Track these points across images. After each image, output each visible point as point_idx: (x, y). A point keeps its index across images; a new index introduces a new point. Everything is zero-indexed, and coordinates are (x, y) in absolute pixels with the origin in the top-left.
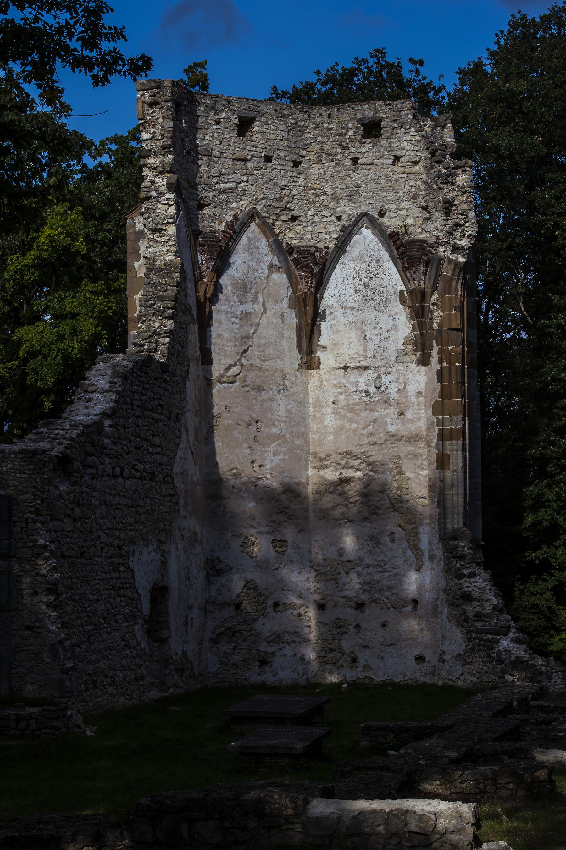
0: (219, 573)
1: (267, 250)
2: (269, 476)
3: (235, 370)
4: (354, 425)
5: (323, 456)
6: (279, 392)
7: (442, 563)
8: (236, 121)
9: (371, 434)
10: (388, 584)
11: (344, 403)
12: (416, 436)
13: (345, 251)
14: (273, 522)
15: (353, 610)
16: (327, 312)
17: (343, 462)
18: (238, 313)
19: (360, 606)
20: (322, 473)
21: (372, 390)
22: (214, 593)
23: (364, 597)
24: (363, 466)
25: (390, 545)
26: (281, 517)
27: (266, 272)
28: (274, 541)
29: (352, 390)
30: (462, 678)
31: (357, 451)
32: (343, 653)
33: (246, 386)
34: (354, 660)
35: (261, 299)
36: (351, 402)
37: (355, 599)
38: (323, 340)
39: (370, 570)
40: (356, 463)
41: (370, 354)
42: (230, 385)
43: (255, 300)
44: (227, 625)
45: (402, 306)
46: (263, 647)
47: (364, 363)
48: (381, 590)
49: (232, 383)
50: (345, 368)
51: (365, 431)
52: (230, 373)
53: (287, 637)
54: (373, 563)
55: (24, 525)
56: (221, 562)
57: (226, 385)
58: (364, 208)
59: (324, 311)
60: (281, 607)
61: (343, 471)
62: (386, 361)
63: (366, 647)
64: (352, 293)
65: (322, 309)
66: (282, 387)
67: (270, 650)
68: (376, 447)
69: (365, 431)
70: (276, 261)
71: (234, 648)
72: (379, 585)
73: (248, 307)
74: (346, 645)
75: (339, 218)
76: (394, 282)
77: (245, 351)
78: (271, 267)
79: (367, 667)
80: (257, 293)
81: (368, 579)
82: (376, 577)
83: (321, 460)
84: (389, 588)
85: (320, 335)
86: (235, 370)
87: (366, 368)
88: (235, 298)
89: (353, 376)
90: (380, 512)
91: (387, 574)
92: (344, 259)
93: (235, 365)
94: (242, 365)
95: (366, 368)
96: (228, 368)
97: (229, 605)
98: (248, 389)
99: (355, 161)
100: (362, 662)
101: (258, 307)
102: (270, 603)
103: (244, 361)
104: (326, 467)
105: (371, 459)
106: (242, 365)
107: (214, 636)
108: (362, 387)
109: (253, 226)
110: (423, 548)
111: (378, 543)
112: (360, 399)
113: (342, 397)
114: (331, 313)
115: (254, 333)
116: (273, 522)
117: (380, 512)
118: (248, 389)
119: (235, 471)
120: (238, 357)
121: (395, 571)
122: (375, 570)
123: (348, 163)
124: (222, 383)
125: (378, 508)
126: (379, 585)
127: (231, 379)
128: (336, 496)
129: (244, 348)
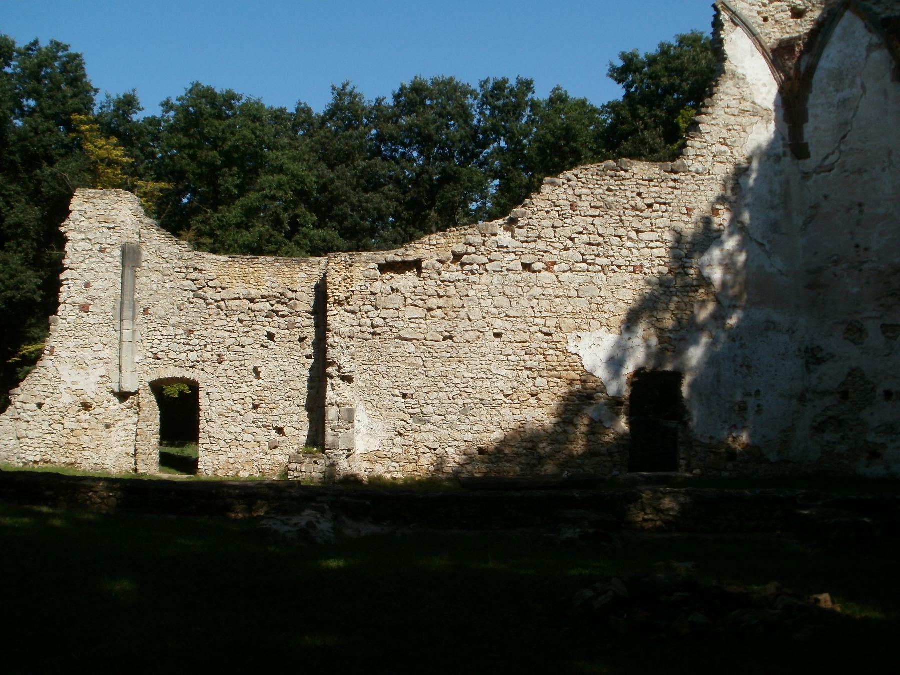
0: (820, 361)
1: (864, 32)
2: (874, 259)
3: (832, 159)
6: (884, 170)
14: (882, 306)
27: (864, 53)
28: (883, 326)
33: (846, 171)
35: (858, 81)
42: (828, 174)
43: (852, 84)
44: (830, 413)
46: (871, 437)
49: (830, 171)
52: (827, 163)
56: (822, 350)
57: (823, 175)
67: (880, 441)
71: (843, 438)
73: (846, 93)
77: (844, 137)
78: (870, 49)
80: (854, 77)
86: (832, 159)
88: (832, 89)
93: (833, 153)
94: (841, 152)
96: (827, 158)
97: (831, 393)
98: (847, 174)
101: (857, 91)
102: (880, 391)
103: (843, 148)
106: (841, 152)
109: (848, 14)
115: (853, 117)
116: (882, 306)
118: (847, 174)
119: (836, 258)
120: (837, 145)
124: (819, 173)
129: (842, 134)
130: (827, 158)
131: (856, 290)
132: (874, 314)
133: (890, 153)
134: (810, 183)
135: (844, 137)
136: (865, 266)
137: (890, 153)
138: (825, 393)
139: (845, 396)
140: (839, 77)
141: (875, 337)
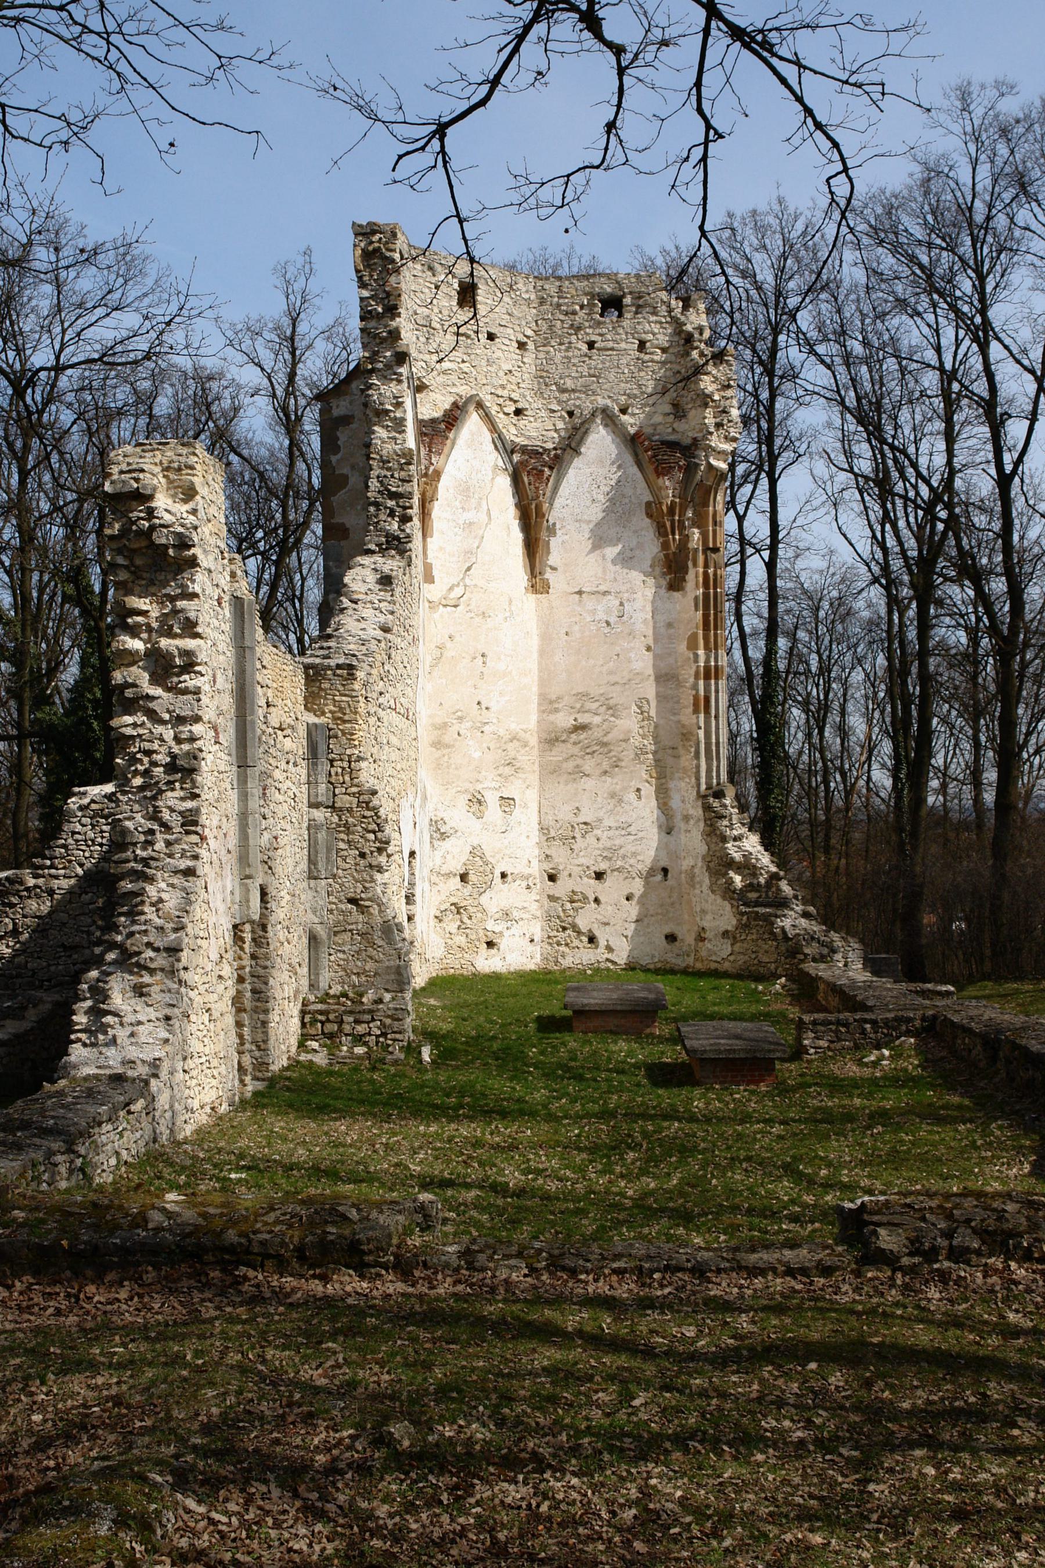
0: (444, 836)
3: (458, 592)
4: (592, 662)
5: (554, 697)
7: (702, 824)
8: (456, 286)
9: (611, 673)
10: (633, 849)
11: (578, 635)
12: (666, 674)
13: (577, 452)
15: (592, 881)
16: (558, 526)
17: (578, 706)
18: (461, 522)
19: (599, 876)
20: (552, 718)
21: (613, 620)
22: (438, 861)
23: (603, 866)
24: (603, 709)
25: (636, 803)
26: (508, 770)
29: (589, 619)
30: (731, 958)
31: (595, 692)
32: (579, 933)
34: (592, 939)
36: (587, 633)
37: (593, 868)
38: (553, 559)
39: (611, 833)
40: (596, 705)
41: (610, 576)
43: (478, 507)
44: (453, 900)
45: (648, 521)
46: (490, 925)
47: (602, 588)
48: (624, 857)
49: (455, 606)
50: (580, 593)
51: (605, 668)
53: (516, 914)
54: (613, 824)
55: (345, 764)
58: (601, 402)
59: (554, 524)
60: (509, 878)
61: (578, 716)
62: (629, 585)
63: (607, 924)
64: (588, 503)
65: (551, 522)
66: (507, 614)
68: (618, 688)
69: (605, 668)
70: (501, 463)
72: (622, 852)
73: (469, 516)
74: (583, 922)
75: (571, 414)
76: (639, 492)
77: (469, 569)
79: (609, 949)
81: (609, 844)
82: (617, 842)
83: (551, 702)
84: (634, 854)
85: (548, 553)
86: (458, 592)
87: (606, 593)
88: (457, 503)
89: (589, 602)
90: (623, 764)
91: (632, 838)
92: (577, 462)
95: (606, 593)
96: (451, 589)
99: (591, 345)
100: (602, 943)
102: (497, 874)
103: (468, 581)
104: (557, 710)
105: (612, 702)
107: (438, 914)
108: (601, 615)
110: (674, 806)
111: (620, 801)
112: (598, 630)
113: (576, 628)
114: (563, 527)
117: (623, 764)
121: (641, 834)
122: (617, 833)
123: (584, 347)
125: (620, 760)
126: (622, 852)
127: (453, 603)
128: (569, 746)
130: (451, 589)
131: (477, 755)
132: (493, 784)
133: (510, 602)
134: (436, 616)
135: (469, 569)
136: (486, 728)
137: (510, 602)
138: (449, 875)
139: (464, 878)
140: (465, 490)
141: (493, 809)
